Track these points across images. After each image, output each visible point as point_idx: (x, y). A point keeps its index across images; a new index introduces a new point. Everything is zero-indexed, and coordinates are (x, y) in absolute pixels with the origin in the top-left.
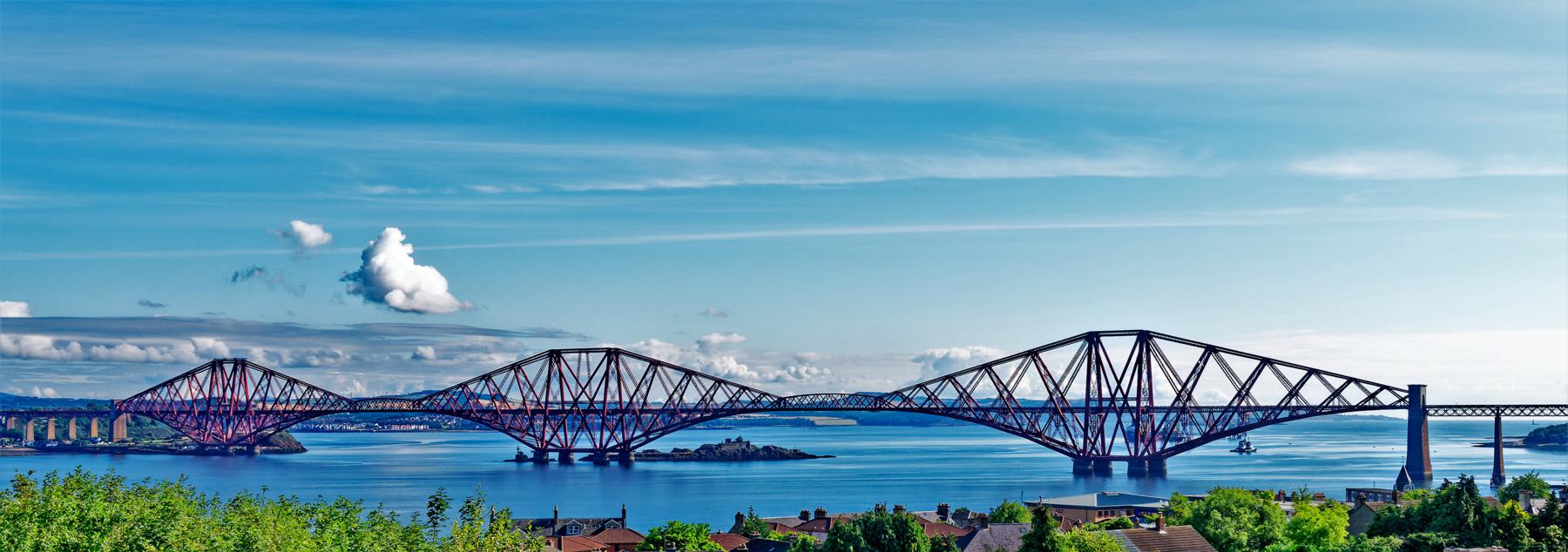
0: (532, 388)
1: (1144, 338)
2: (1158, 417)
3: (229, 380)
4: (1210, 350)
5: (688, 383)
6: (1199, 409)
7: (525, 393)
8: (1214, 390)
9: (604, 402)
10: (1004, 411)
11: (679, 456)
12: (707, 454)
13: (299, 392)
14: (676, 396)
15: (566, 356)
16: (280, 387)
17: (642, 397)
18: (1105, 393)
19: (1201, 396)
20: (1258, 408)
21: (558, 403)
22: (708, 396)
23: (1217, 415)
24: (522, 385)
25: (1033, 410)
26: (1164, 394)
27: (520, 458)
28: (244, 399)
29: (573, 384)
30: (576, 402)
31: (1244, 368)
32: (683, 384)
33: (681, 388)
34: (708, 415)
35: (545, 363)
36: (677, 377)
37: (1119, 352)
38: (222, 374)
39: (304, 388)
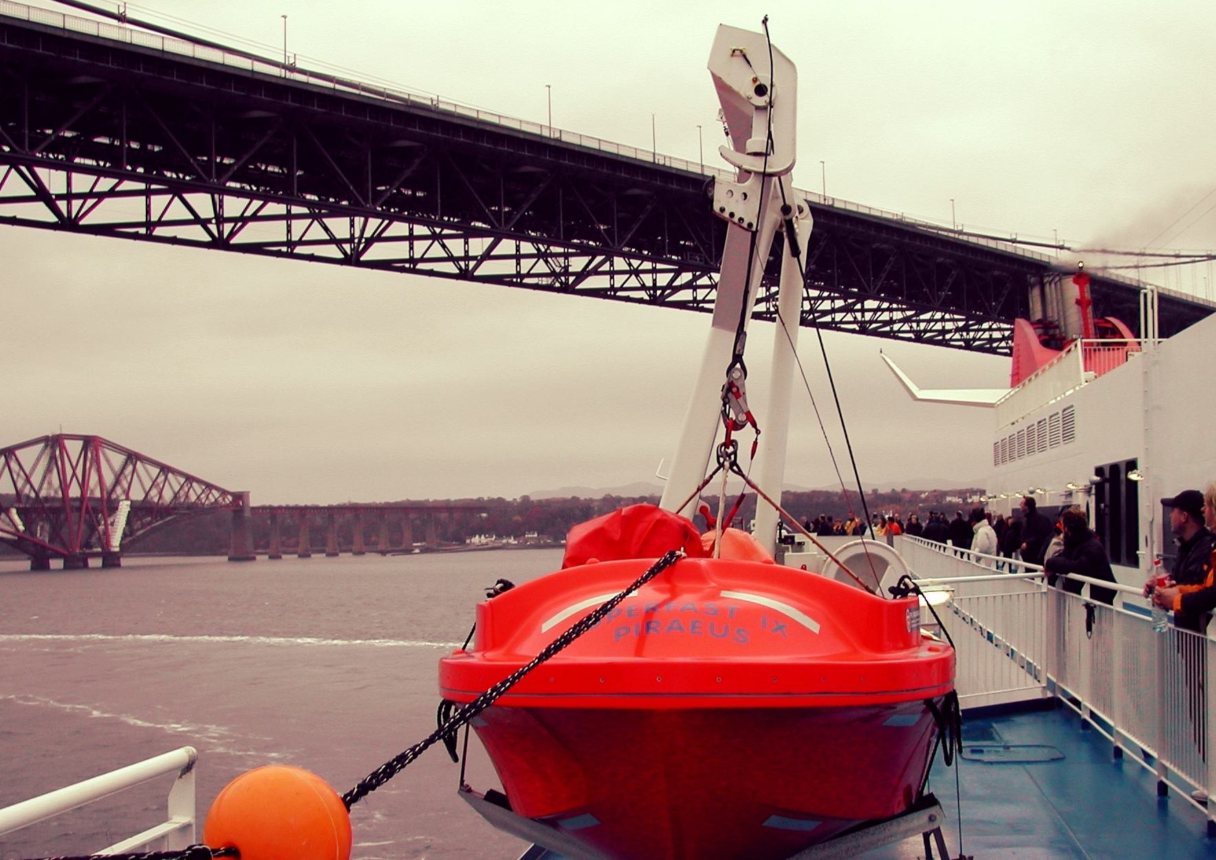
0: (28, 480)
3: (74, 469)
5: (157, 478)
7: (20, 484)
13: (175, 482)
14: (154, 492)
15: (67, 443)
16: (151, 478)
17: (124, 491)
21: (58, 499)
22: (182, 493)
24: (15, 476)
28: (33, 495)
32: (159, 480)
33: (158, 484)
35: (42, 453)
36: (155, 471)
38: (61, 453)
39: (182, 480)
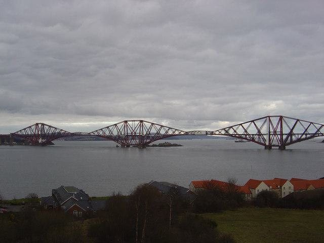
1: (281, 118)
2: (284, 137)
4: (298, 120)
6: (294, 134)
8: (298, 130)
9: (140, 133)
10: (246, 135)
11: (154, 146)
12: (161, 145)
18: (272, 130)
19: (294, 131)
20: (309, 134)
23: (300, 136)
25: (253, 135)
26: (286, 130)
27: (117, 146)
29: (131, 130)
30: (132, 133)
31: (306, 125)
34: (166, 136)
37: (275, 121)
